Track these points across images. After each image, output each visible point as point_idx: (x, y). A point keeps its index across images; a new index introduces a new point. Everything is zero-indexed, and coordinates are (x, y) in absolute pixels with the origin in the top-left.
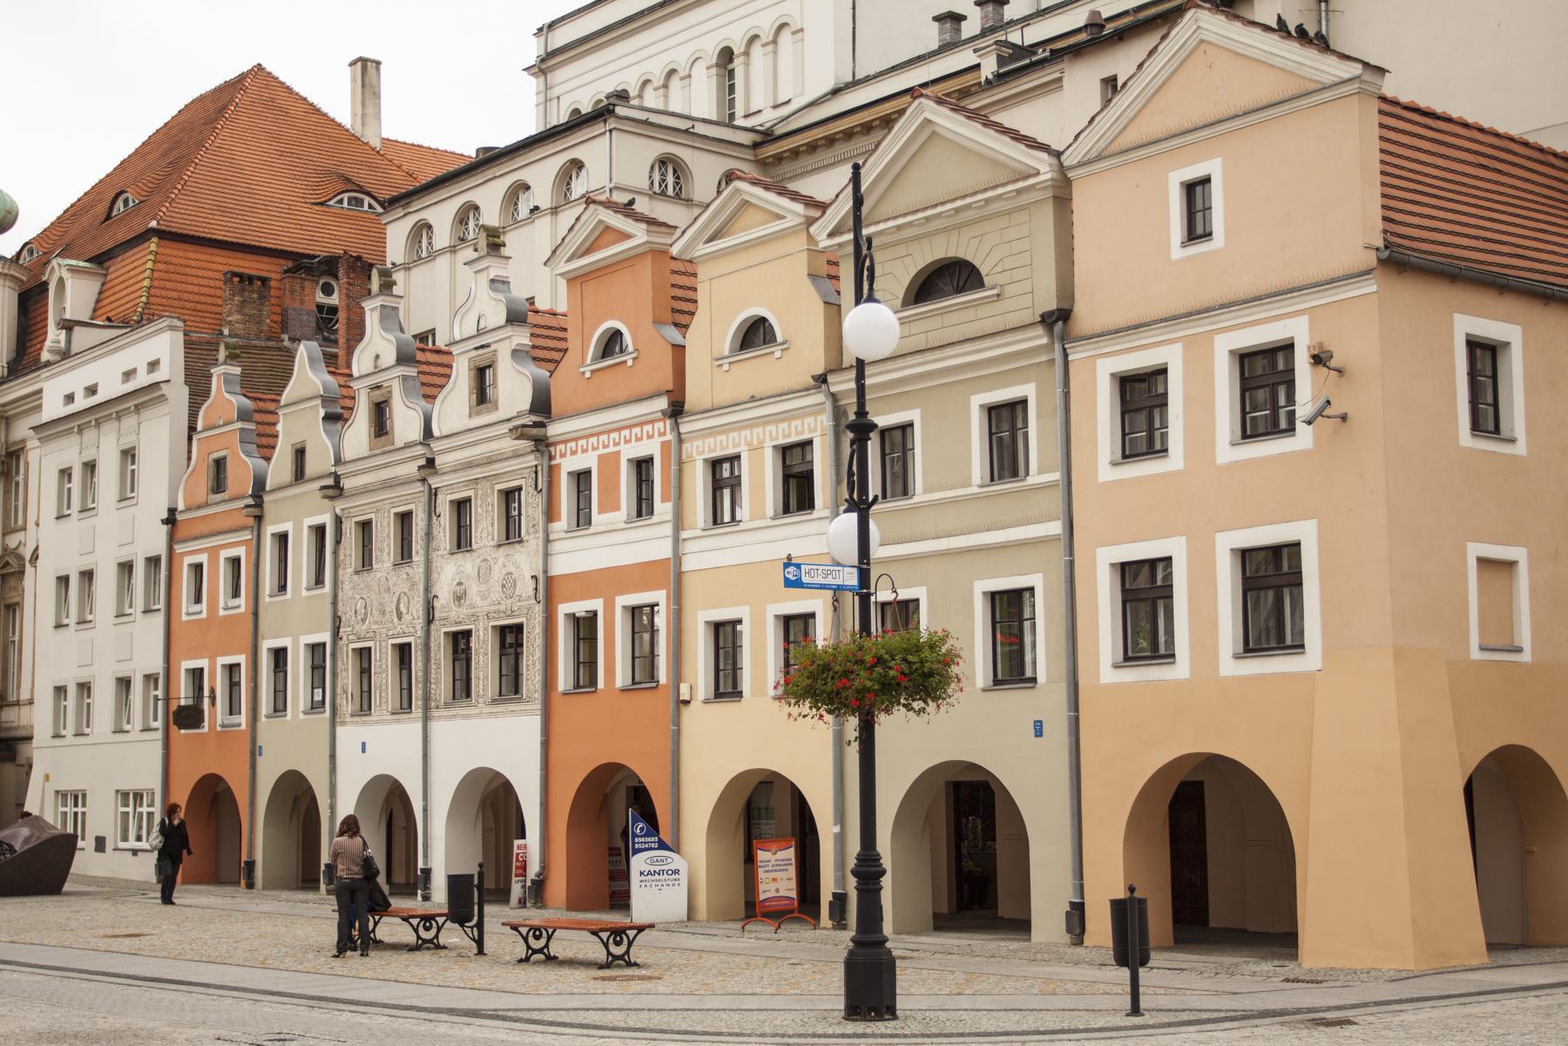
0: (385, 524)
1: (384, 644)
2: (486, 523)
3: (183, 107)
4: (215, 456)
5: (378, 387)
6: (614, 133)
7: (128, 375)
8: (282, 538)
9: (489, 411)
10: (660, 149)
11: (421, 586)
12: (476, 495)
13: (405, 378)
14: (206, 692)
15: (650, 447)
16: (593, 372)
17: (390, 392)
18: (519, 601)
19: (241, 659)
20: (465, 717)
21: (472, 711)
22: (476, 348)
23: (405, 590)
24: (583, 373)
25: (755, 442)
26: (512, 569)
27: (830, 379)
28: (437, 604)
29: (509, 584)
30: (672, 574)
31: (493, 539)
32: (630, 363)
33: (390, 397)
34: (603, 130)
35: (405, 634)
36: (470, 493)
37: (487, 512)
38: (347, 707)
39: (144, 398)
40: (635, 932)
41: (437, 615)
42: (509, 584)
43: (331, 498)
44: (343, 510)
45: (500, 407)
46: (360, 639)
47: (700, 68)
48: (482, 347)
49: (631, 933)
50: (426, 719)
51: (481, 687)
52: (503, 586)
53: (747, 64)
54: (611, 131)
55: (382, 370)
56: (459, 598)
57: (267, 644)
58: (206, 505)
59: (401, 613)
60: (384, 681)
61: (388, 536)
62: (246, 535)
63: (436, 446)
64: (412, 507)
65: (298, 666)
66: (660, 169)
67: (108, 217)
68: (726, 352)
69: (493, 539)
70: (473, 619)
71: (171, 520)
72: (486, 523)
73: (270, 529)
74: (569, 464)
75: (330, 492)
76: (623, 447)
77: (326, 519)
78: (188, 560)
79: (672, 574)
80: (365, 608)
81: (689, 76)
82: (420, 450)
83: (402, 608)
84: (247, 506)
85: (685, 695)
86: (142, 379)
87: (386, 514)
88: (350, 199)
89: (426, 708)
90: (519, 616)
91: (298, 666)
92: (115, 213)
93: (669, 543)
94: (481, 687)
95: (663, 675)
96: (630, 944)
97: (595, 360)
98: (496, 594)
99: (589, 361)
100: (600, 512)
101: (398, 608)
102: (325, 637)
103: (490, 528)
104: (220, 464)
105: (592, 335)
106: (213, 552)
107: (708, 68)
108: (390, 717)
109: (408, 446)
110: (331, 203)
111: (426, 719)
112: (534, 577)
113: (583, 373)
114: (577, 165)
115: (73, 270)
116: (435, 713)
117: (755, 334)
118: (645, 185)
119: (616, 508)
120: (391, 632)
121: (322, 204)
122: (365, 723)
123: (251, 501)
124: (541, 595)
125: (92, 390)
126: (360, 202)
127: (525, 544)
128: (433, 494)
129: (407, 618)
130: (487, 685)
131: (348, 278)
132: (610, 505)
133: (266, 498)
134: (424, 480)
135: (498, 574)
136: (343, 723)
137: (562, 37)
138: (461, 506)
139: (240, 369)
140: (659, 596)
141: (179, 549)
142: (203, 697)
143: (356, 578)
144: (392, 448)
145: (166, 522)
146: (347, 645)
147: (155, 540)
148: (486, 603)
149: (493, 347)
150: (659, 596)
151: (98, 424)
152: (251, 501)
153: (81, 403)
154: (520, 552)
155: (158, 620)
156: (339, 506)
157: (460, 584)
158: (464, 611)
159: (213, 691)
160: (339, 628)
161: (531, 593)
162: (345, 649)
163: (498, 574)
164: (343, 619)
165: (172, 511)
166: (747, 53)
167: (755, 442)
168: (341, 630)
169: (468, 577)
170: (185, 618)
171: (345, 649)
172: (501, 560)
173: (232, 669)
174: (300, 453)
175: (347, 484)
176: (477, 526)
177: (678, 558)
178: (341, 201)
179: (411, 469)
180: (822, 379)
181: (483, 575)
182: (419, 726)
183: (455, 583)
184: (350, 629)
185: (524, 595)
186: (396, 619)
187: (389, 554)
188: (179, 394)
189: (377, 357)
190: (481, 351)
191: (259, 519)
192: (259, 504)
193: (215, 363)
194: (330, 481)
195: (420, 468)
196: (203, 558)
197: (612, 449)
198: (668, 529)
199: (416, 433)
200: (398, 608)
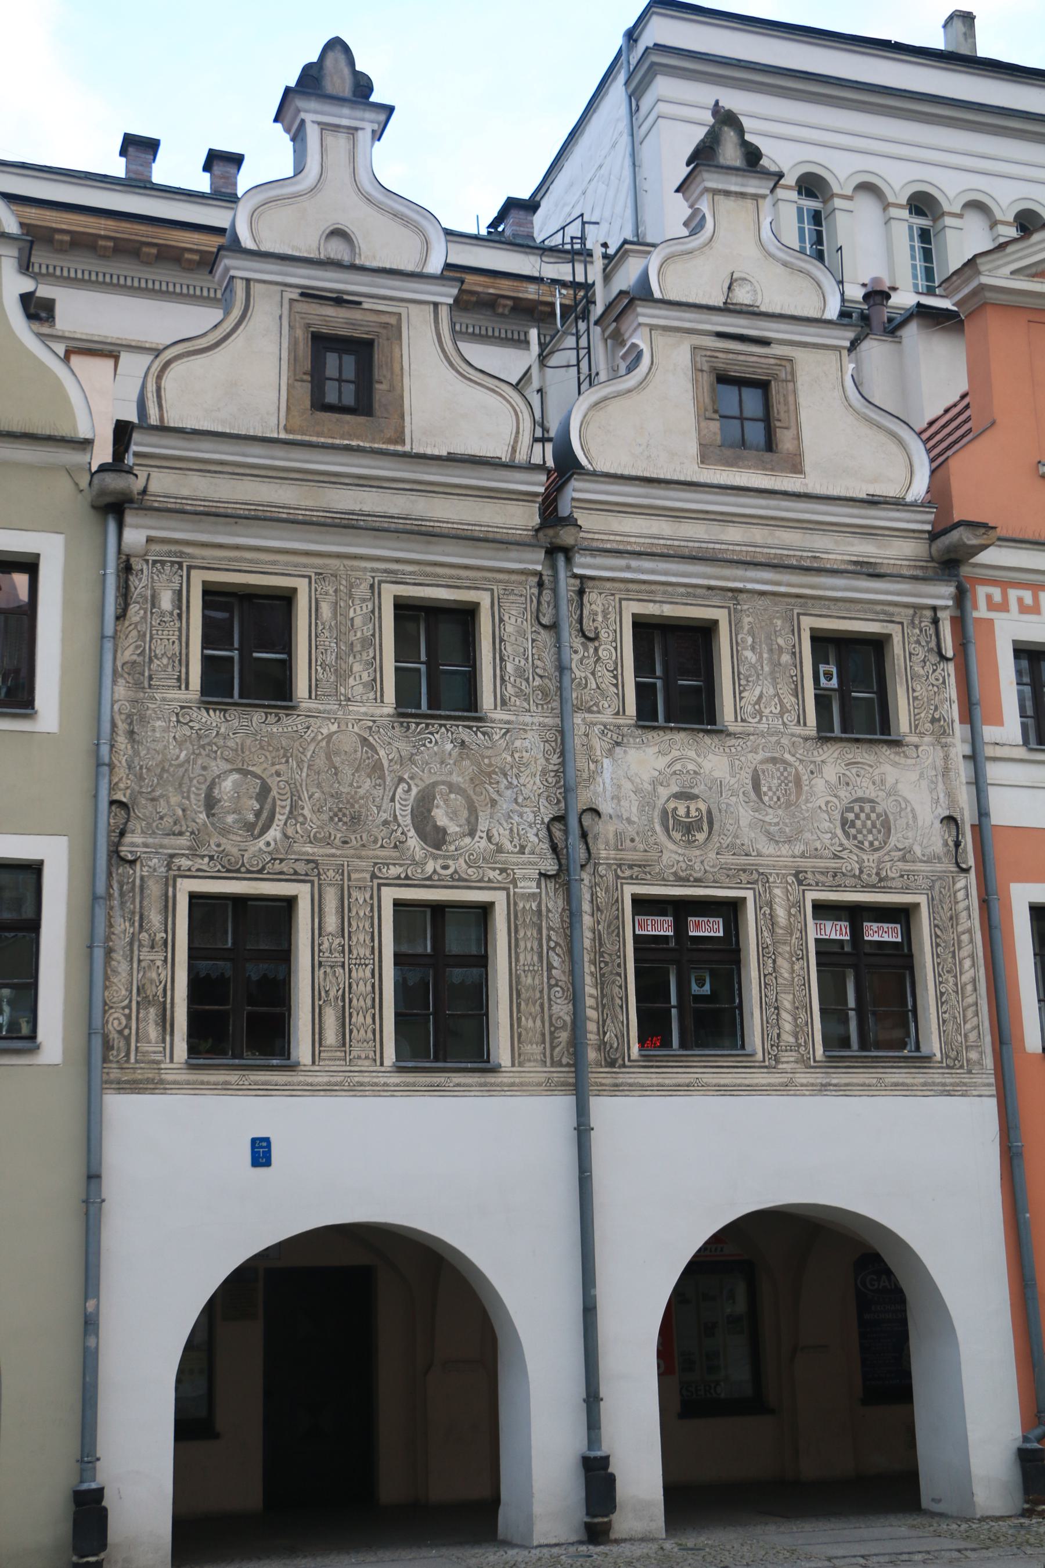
0: (358, 612)
1: (359, 896)
5: (339, 300)
11: (532, 783)
12: (735, 626)
18: (903, 859)
20: (723, 1090)
21: (761, 1078)
22: (720, 335)
23: (455, 778)
26: (871, 792)
31: (801, 721)
35: (458, 881)
37: (776, 664)
41: (603, 852)
45: (807, 467)
46: (232, 872)
51: (787, 1027)
52: (844, 822)
55: (363, 269)
59: (444, 831)
60: (362, 988)
61: (372, 641)
69: (801, 721)
70: (744, 877)
80: (265, 791)
83: (440, 817)
87: (362, 590)
94: (787, 1027)
103: (789, 700)
108: (396, 1079)
112: (950, 820)
120: (394, 871)
122: (266, 1090)
124: (971, 862)
127: (911, 751)
130: (765, 1023)
143: (214, 718)
144: (399, 448)
146: (169, 882)
148: (798, 849)
149: (776, 350)
154: (895, 764)
157: (683, 796)
160: (122, 834)
162: (154, 889)
164: (143, 809)
168: (128, 839)
171: (154, 889)
172: (831, 772)
183: (664, 793)
184: (184, 841)
185: (918, 850)
186: (413, 842)
187: (375, 684)
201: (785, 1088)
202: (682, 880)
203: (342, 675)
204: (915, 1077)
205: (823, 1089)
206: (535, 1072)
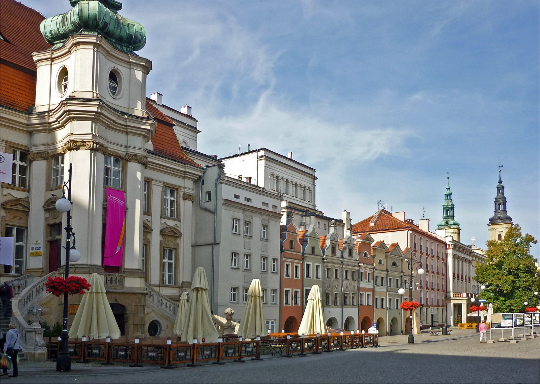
2: (350, 276)
5: (334, 244)
8: (308, 265)
9: (351, 257)
11: (340, 284)
15: (370, 272)
20: (348, 308)
21: (349, 307)
29: (354, 287)
30: (373, 290)
36: (348, 270)
42: (354, 287)
48: (351, 246)
64: (339, 269)
72: (350, 276)
73: (306, 263)
74: (361, 271)
78: (285, 263)
79: (373, 290)
95: (371, 304)
98: (352, 288)
101: (336, 287)
106: (293, 263)
109: (338, 257)
112: (358, 287)
116: (344, 306)
135: (352, 285)
136: (325, 307)
138: (346, 271)
140: (371, 293)
150: (371, 293)
155: (278, 277)
157: (347, 285)
158: (347, 290)
161: (357, 289)
163: (352, 285)
169: (348, 284)
173: (296, 292)
181: (350, 284)
191: (303, 259)
196: (290, 264)
197: (366, 270)
201: (350, 308)
202: (346, 292)
203: (333, 275)
204: (354, 307)
205: (352, 308)
206: (340, 306)
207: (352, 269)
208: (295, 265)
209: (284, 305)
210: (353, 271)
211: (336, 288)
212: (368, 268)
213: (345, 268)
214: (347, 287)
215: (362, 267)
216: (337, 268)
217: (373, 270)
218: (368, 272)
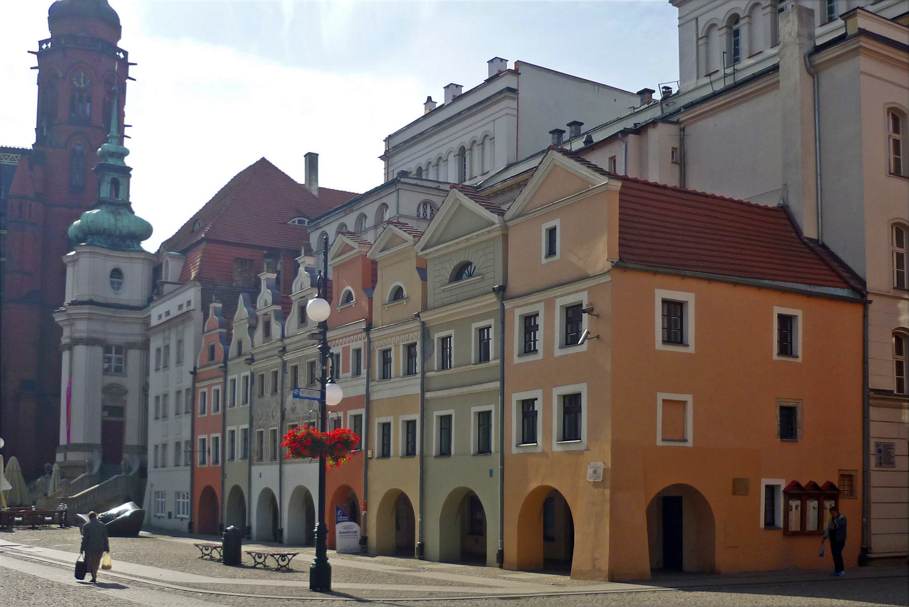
3: (233, 177)
4: (211, 344)
5: (266, 314)
6: (399, 190)
7: (180, 307)
8: (234, 381)
10: (422, 197)
13: (275, 311)
14: (207, 450)
15: (361, 344)
16: (341, 309)
17: (270, 317)
19: (219, 435)
24: (338, 310)
25: (397, 343)
27: (421, 315)
28: (287, 412)
32: (354, 306)
33: (270, 319)
34: (395, 189)
38: (255, 458)
39: (184, 317)
40: (292, 556)
43: (250, 364)
44: (254, 369)
47: (452, 155)
49: (290, 557)
50: (281, 464)
53: (471, 155)
54: (398, 190)
56: (293, 410)
57: (229, 428)
58: (208, 365)
62: (221, 380)
63: (287, 341)
65: (267, 438)
66: (423, 207)
67: (193, 231)
68: (387, 302)
71: (194, 373)
73: (230, 377)
75: (248, 361)
76: (350, 344)
77: (248, 373)
78: (200, 391)
81: (447, 160)
82: (280, 344)
84: (221, 367)
85: (370, 455)
86: (185, 309)
88: (299, 220)
89: (281, 459)
90: (314, 419)
91: (267, 438)
92: (195, 229)
93: (364, 388)
96: (289, 561)
97: (343, 304)
99: (340, 305)
100: (343, 372)
102: (247, 426)
104: (212, 348)
105: (341, 293)
107: (455, 156)
110: (289, 223)
111: (281, 464)
113: (338, 310)
114: (385, 206)
115: (172, 257)
117: (398, 294)
118: (415, 213)
119: (349, 372)
121: (285, 223)
122: (261, 465)
123: (222, 365)
125: (168, 313)
126: (303, 222)
128: (284, 363)
129: (276, 418)
131: (284, 259)
132: (346, 370)
133: (229, 363)
134: (281, 357)
136: (254, 465)
137: (395, 142)
139: (221, 305)
141: (198, 385)
142: (206, 451)
145: (192, 373)
147: (188, 381)
151: (169, 329)
152: (222, 365)
153: (164, 319)
156: (252, 368)
157: (294, 404)
159: (209, 449)
160: (252, 422)
165: (195, 368)
166: (471, 149)
167: (397, 343)
170: (199, 416)
174: (240, 344)
175: (256, 357)
176: (300, 378)
177: (368, 395)
178: (294, 222)
179: (276, 352)
180: (418, 315)
182: (277, 467)
188: (198, 315)
189: (266, 301)
190: (302, 299)
191: (226, 372)
192: (226, 365)
193: (211, 302)
194: (249, 357)
195: (280, 351)
196: (206, 390)
197: (347, 345)
198: (365, 381)
199: (279, 336)
200: (273, 414)
207: (306, 357)
208: (214, 388)
209: (199, 466)
210: (293, 364)
211: (273, 417)
212: (353, 335)
213: (292, 361)
214: (293, 410)
215: (332, 341)
216: (275, 369)
217: (364, 334)
218: (354, 345)
